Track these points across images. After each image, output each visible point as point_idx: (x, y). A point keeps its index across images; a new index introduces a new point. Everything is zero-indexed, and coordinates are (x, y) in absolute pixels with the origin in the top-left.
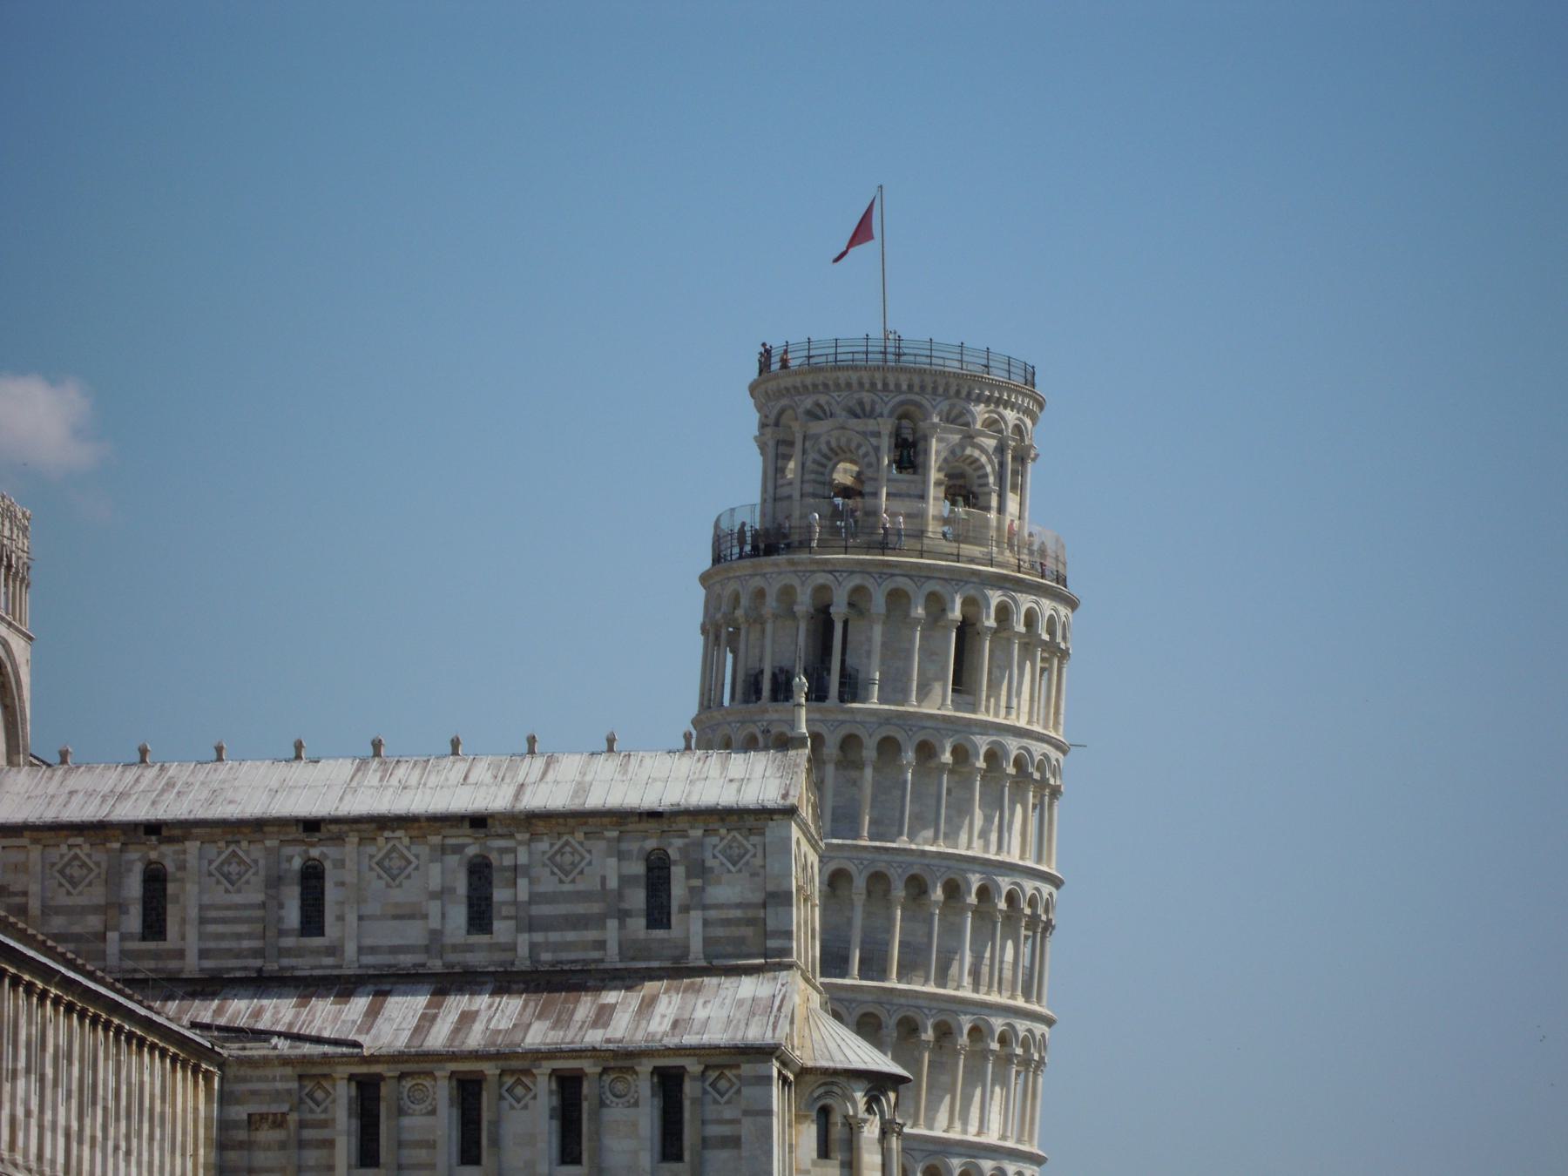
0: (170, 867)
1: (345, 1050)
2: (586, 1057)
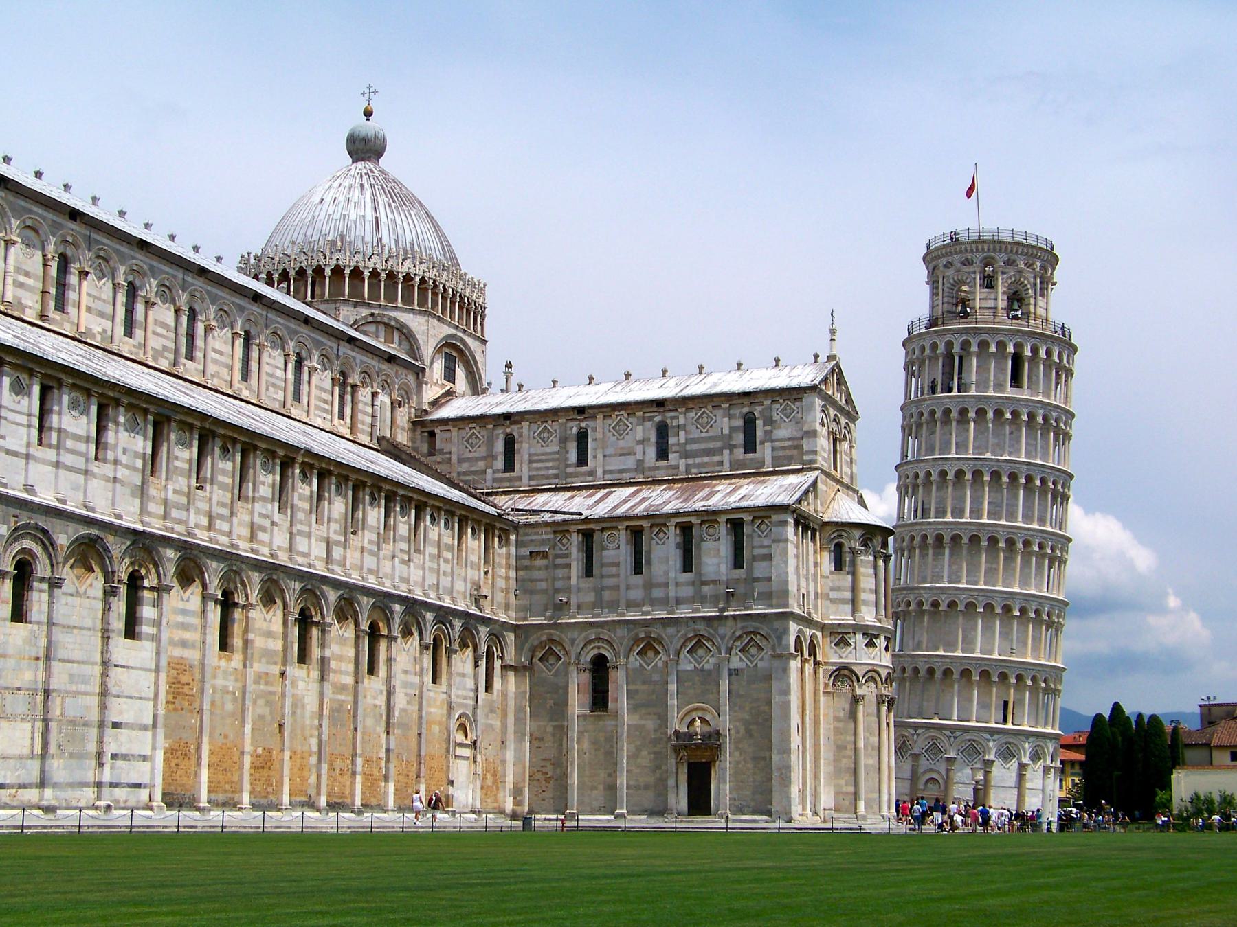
0: (516, 436)
1: (574, 517)
2: (693, 515)
